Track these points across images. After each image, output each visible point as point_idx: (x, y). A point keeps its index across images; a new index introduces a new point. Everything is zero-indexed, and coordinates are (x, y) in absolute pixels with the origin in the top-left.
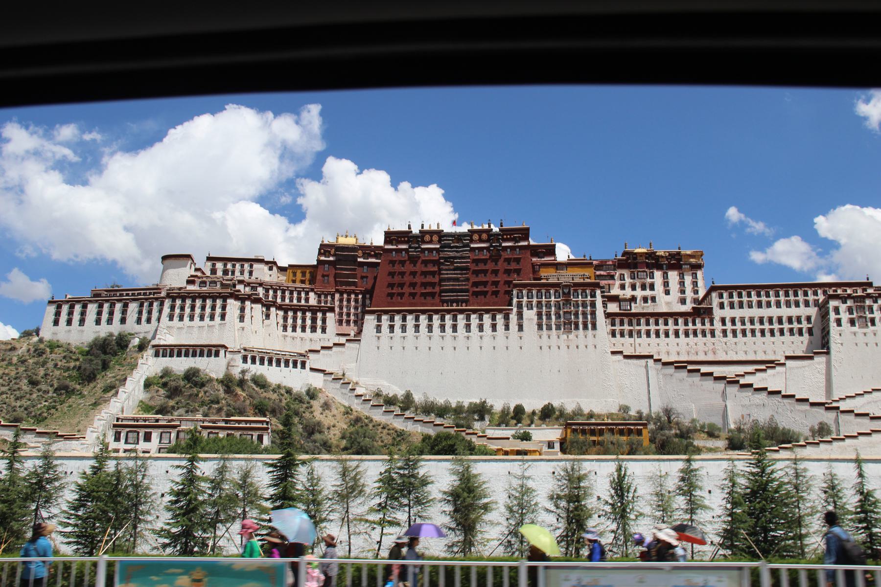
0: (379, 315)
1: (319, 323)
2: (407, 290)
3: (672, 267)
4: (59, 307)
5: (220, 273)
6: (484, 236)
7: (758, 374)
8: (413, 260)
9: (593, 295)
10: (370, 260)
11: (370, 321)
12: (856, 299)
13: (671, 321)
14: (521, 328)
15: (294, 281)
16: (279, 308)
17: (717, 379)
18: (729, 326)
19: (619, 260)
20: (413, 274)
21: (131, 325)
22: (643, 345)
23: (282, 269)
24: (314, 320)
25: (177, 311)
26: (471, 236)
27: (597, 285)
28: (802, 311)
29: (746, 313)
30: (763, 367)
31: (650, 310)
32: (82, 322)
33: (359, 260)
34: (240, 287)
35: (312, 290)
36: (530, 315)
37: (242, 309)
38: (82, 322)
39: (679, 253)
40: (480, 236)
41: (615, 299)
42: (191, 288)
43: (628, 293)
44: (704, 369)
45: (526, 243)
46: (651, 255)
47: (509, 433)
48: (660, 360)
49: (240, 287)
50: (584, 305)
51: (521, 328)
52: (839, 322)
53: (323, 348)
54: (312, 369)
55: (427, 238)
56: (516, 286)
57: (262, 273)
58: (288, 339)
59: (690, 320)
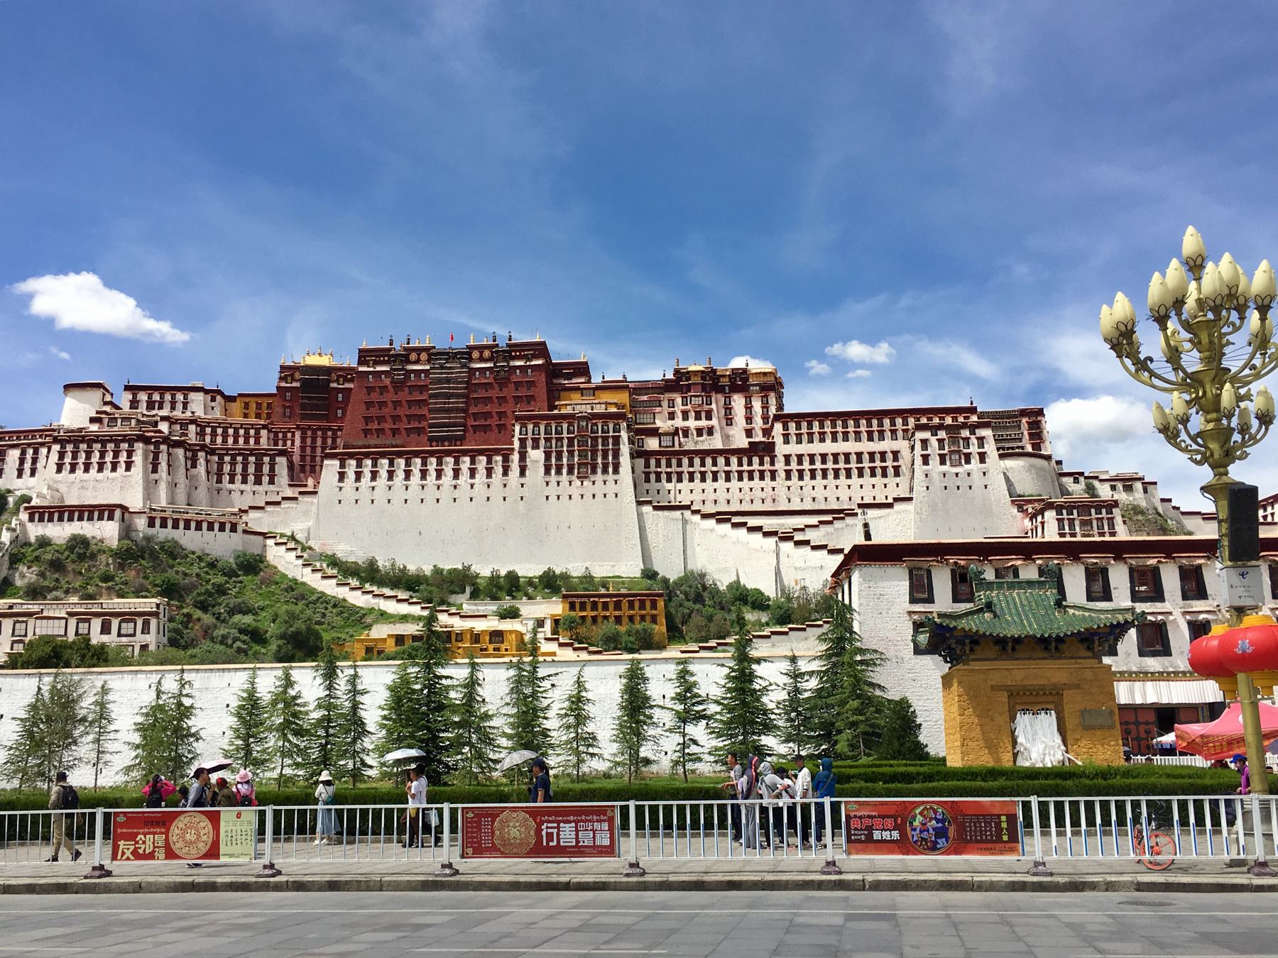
1: (266, 469)
2: (388, 426)
3: (735, 389)
5: (143, 408)
6: (487, 354)
7: (823, 529)
8: (398, 386)
9: (617, 430)
11: (331, 466)
12: (948, 428)
14: (522, 473)
15: (246, 416)
17: (767, 534)
18: (794, 466)
19: (667, 381)
20: (397, 404)
22: (684, 492)
24: (259, 467)
25: (68, 460)
26: (470, 354)
27: (622, 416)
28: (887, 445)
29: (817, 448)
30: (829, 518)
31: (705, 447)
33: (334, 385)
34: (164, 427)
35: (264, 427)
36: (537, 455)
37: (156, 457)
39: (745, 371)
40: (481, 353)
41: (654, 432)
42: (95, 427)
43: (679, 422)
44: (753, 522)
45: (540, 362)
47: (492, 607)
48: (697, 512)
49: (164, 427)
51: (522, 473)
52: (926, 460)
53: (268, 503)
54: (245, 532)
55: (413, 356)
56: (518, 419)
57: (197, 405)
58: (224, 493)
59: (745, 460)
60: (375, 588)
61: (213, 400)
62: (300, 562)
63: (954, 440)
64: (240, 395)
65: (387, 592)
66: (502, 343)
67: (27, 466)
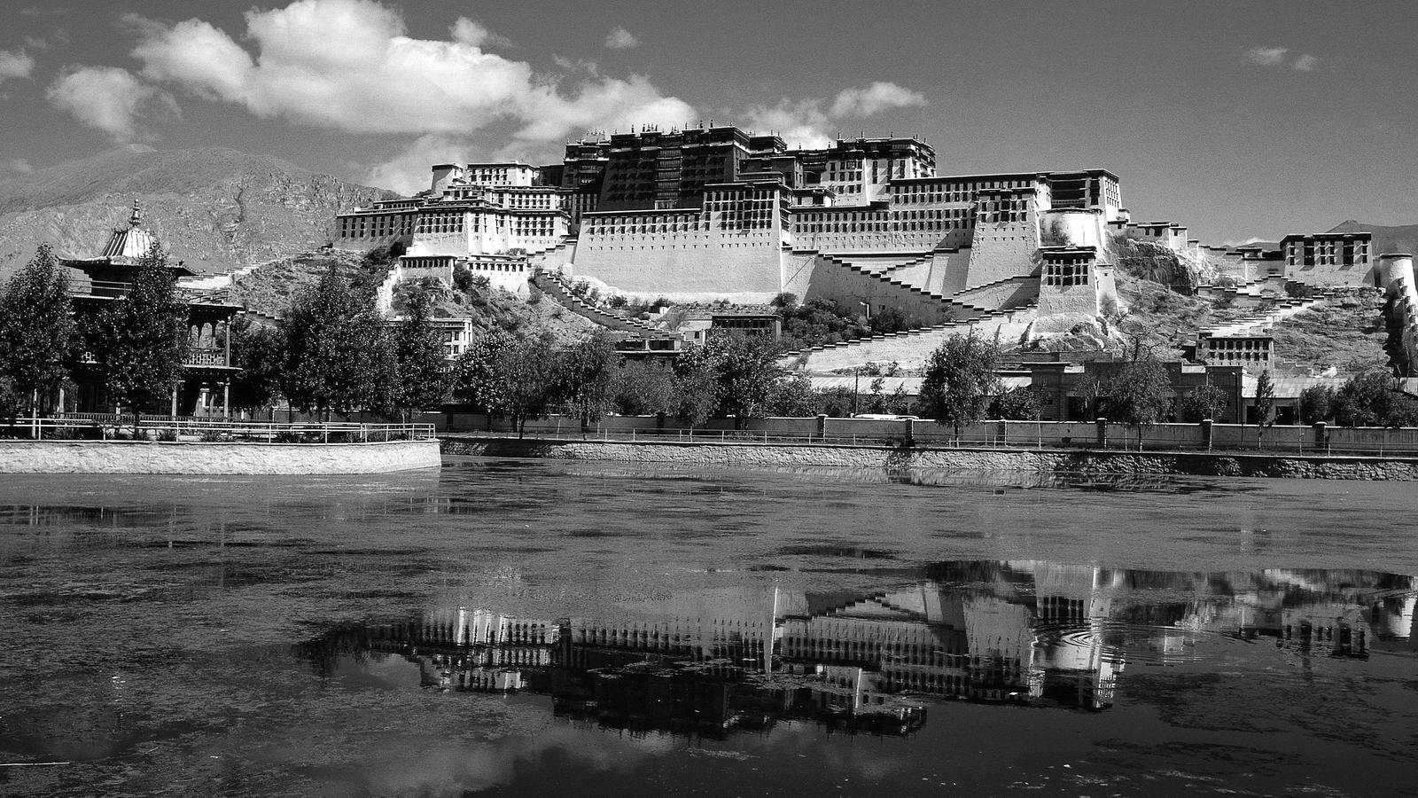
0: (593, 218)
1: (548, 227)
3: (880, 156)
4: (345, 221)
11: (585, 226)
13: (850, 215)
16: (515, 214)
28: (967, 205)
35: (553, 193)
46: (861, 144)
50: (763, 206)
61: (523, 172)
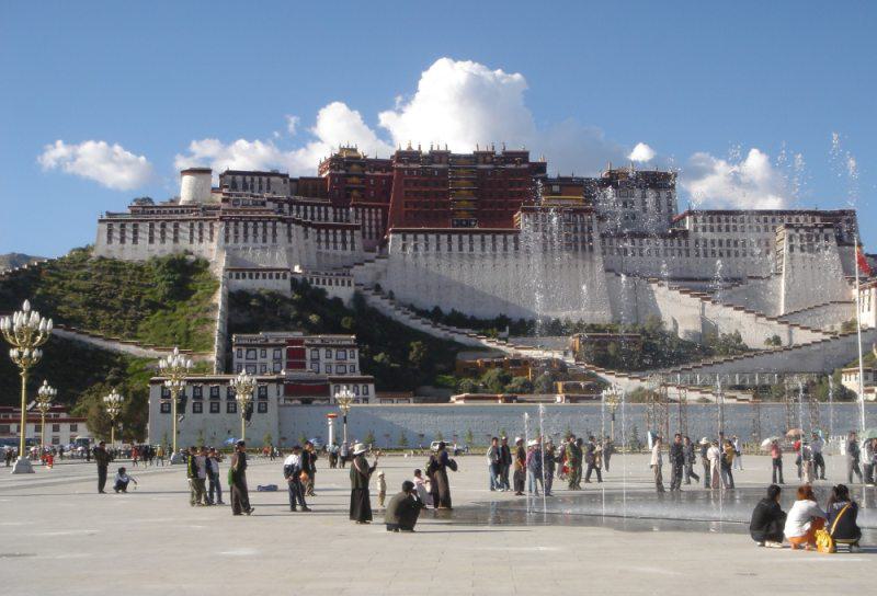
1: (348, 239)
10: (378, 173)
12: (807, 229)
16: (314, 226)
21: (184, 244)
23: (292, 180)
24: (344, 234)
32: (135, 240)
33: (368, 173)
38: (135, 240)
45: (526, 166)
49: (270, 205)
60: (445, 327)
62: (393, 307)
63: (809, 238)
64: (301, 178)
65: (454, 328)
66: (499, 152)
67: (196, 235)
